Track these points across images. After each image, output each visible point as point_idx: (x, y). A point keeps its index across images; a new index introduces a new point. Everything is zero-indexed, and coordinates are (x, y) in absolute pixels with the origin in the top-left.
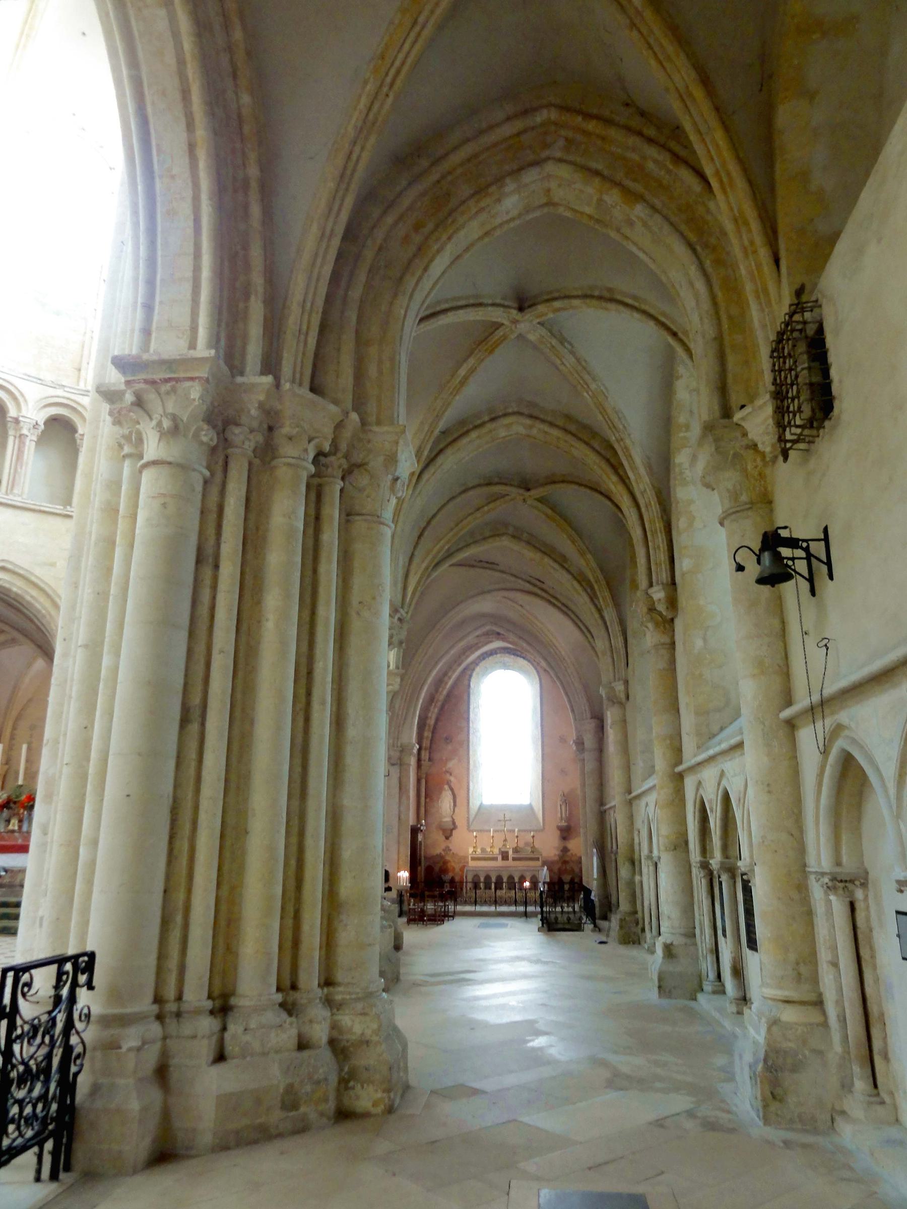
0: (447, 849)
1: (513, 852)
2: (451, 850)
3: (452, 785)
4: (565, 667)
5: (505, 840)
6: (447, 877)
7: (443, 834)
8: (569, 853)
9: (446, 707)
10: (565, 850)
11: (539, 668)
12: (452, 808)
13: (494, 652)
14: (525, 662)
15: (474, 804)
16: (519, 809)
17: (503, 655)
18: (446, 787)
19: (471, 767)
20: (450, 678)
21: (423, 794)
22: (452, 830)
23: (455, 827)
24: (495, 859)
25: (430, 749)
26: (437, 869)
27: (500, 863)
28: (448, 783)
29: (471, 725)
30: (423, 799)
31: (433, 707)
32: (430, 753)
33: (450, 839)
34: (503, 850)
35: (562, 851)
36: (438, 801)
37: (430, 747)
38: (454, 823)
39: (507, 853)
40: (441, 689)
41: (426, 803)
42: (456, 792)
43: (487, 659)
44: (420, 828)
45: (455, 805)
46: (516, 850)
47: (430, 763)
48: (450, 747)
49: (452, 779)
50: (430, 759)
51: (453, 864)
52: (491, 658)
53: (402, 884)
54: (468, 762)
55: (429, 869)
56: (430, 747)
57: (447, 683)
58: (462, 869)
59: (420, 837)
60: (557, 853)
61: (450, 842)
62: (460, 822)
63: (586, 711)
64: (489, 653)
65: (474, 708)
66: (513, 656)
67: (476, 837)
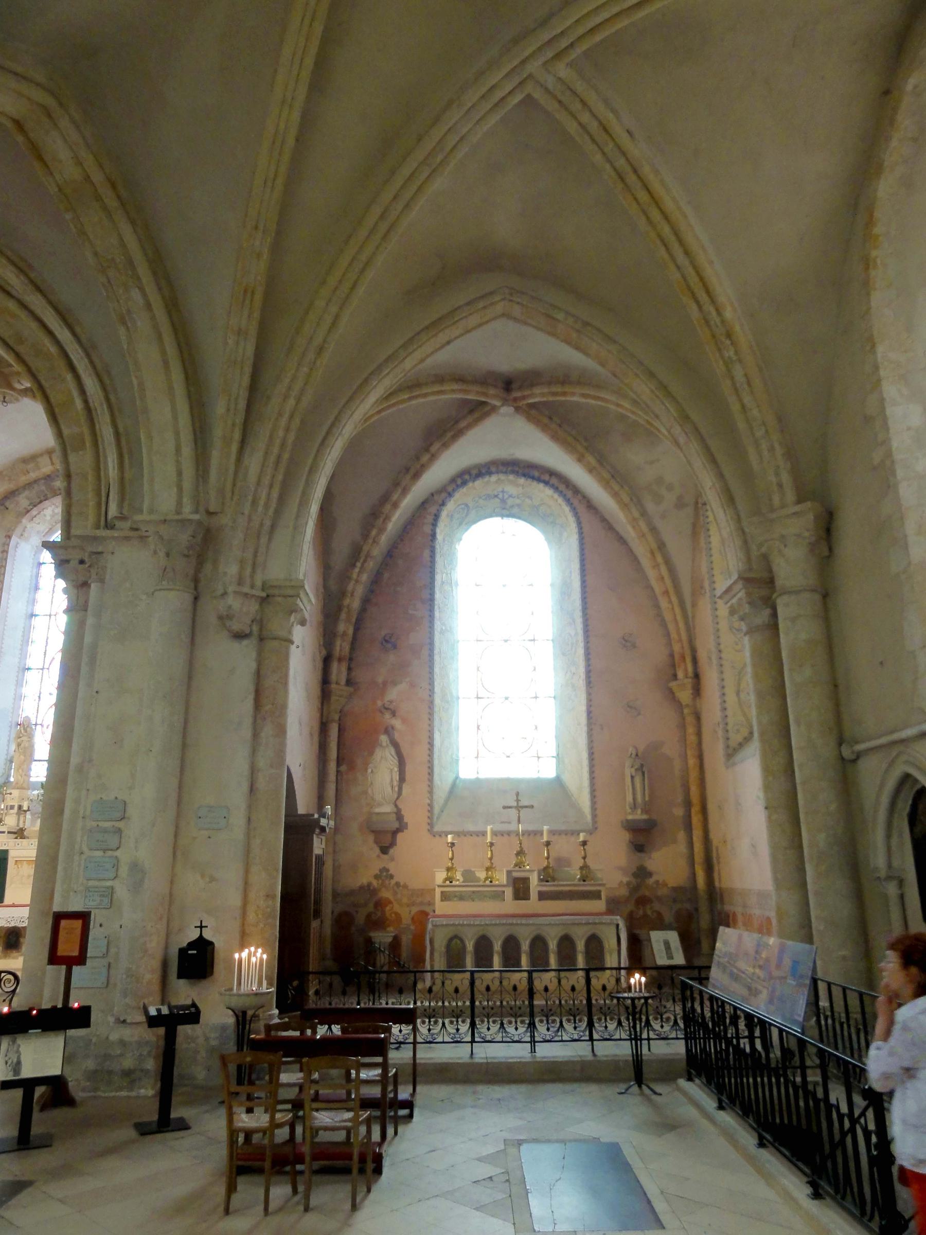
0: (384, 874)
1: (540, 880)
2: (392, 877)
3: (397, 736)
4: (728, 363)
5: (520, 853)
6: (382, 938)
7: (376, 842)
8: (651, 881)
9: (386, 575)
10: (642, 873)
11: (575, 502)
12: (395, 783)
14: (549, 492)
15: (443, 780)
16: (538, 785)
17: (502, 477)
18: (384, 739)
19: (437, 700)
20: (395, 505)
21: (333, 753)
22: (395, 833)
23: (402, 827)
24: (499, 896)
25: (351, 661)
26: (360, 919)
27: (510, 905)
28: (388, 731)
29: (437, 614)
30: (332, 766)
31: (357, 570)
32: (349, 669)
33: (391, 851)
34: (515, 874)
35: (635, 875)
36: (366, 770)
37: (351, 659)
38: (399, 816)
39: (526, 881)
40: (374, 533)
42: (405, 751)
43: (471, 484)
44: (318, 821)
45: (402, 779)
46: (547, 875)
47: (351, 689)
48: (392, 658)
49: (397, 723)
50: (349, 682)
51: (397, 908)
52: (479, 483)
53: (244, 989)
54: (431, 683)
55: (343, 921)
56: (351, 659)
57: (387, 518)
58: (422, 917)
59: (318, 846)
60: (625, 880)
61: (392, 859)
62: (414, 817)
63: (780, 485)
64: (474, 472)
65: (443, 583)
66: (522, 480)
67: (453, 844)
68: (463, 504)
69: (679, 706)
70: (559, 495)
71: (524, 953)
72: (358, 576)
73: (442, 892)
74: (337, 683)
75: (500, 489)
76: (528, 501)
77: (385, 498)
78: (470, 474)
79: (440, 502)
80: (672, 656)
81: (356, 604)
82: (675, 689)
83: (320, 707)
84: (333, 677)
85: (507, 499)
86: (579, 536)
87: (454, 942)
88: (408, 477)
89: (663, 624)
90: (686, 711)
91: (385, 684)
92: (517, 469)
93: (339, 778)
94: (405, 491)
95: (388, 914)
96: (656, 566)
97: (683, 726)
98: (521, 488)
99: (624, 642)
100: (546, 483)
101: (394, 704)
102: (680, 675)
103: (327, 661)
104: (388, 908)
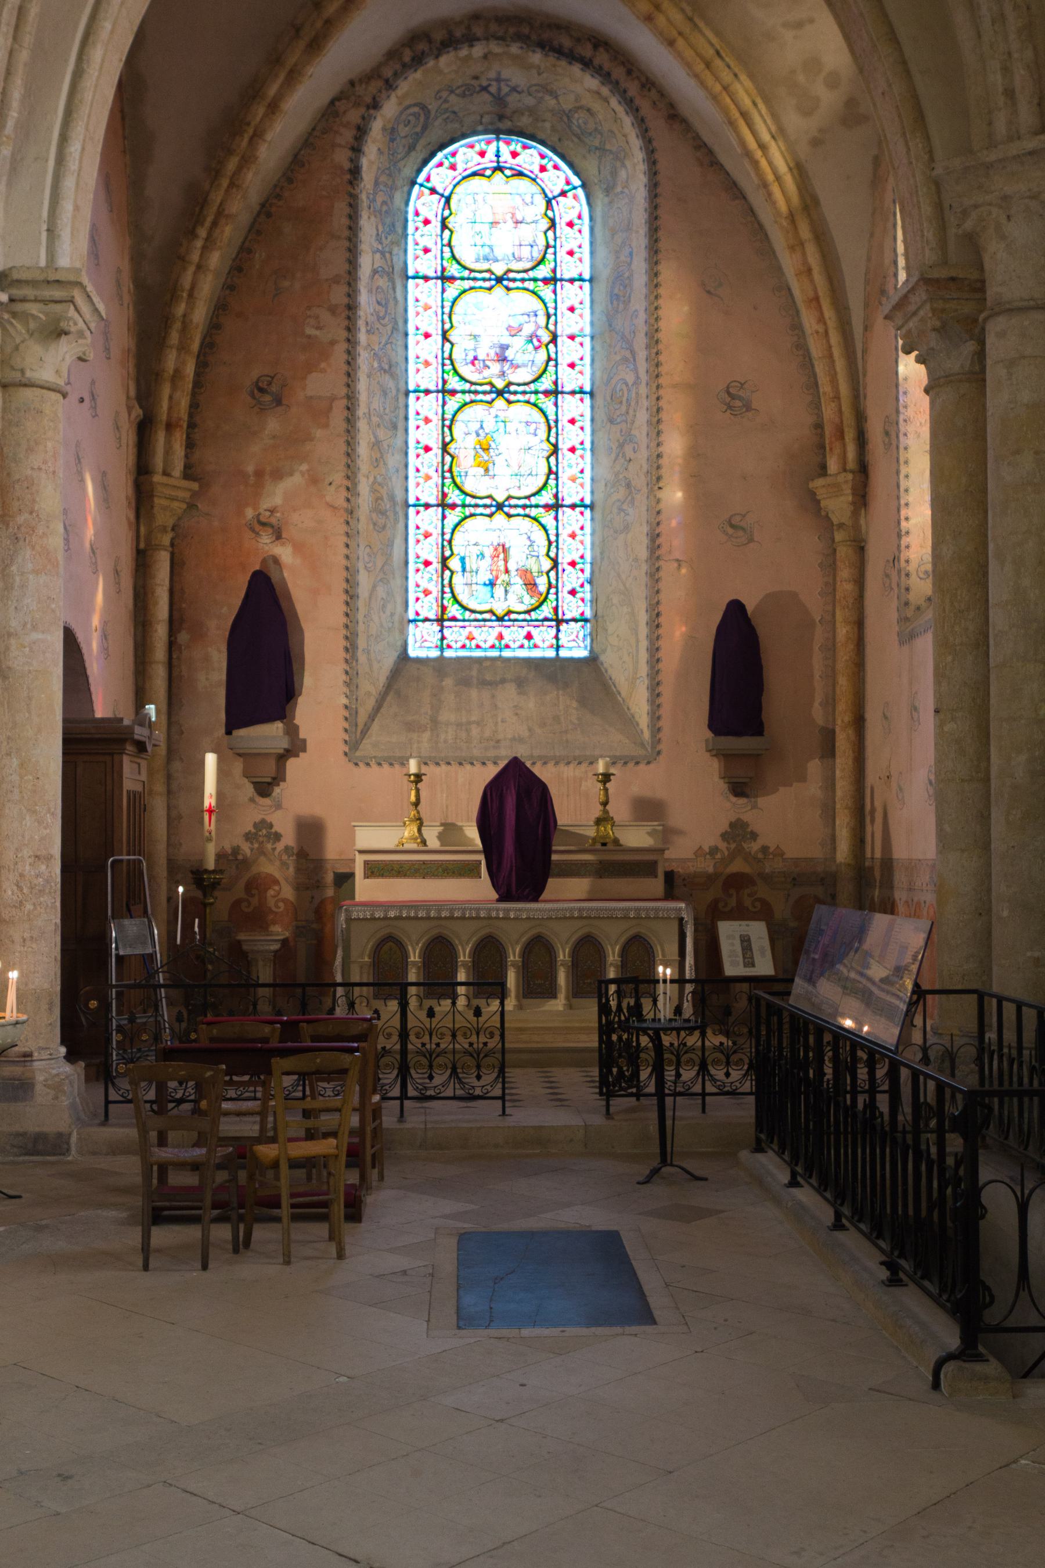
7: (246, 775)
11: (646, 109)
13: (458, 34)
14: (591, 82)
17: (496, 48)
21: (161, 610)
30: (160, 632)
31: (199, 244)
32: (190, 445)
33: (277, 790)
35: (724, 836)
40: (232, 164)
41: (172, 644)
47: (195, 486)
48: (273, 425)
50: (189, 473)
61: (278, 806)
63: (1010, 93)
64: (438, 36)
66: (536, 57)
68: (415, 105)
69: (826, 524)
70: (611, 91)
71: (513, 965)
72: (201, 256)
73: (366, 863)
74: (166, 473)
75: (492, 74)
76: (552, 102)
77: (252, 92)
78: (430, 41)
79: (368, 99)
80: (819, 426)
81: (200, 315)
82: (821, 494)
83: (132, 516)
84: (158, 461)
85: (507, 95)
86: (650, 180)
87: (386, 948)
88: (302, 44)
89: (807, 363)
90: (839, 536)
91: (259, 474)
92: (526, 30)
93: (175, 656)
94: (293, 77)
95: (271, 903)
96: (797, 245)
97: (830, 565)
98: (534, 72)
99: (728, 399)
100: (587, 64)
101: (278, 515)
102: (833, 466)
103: (144, 429)
104: (271, 892)
